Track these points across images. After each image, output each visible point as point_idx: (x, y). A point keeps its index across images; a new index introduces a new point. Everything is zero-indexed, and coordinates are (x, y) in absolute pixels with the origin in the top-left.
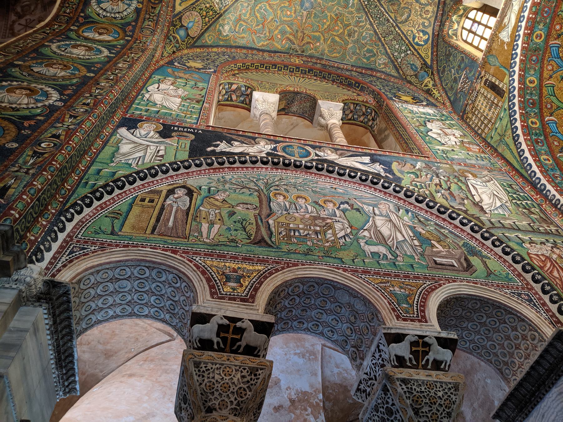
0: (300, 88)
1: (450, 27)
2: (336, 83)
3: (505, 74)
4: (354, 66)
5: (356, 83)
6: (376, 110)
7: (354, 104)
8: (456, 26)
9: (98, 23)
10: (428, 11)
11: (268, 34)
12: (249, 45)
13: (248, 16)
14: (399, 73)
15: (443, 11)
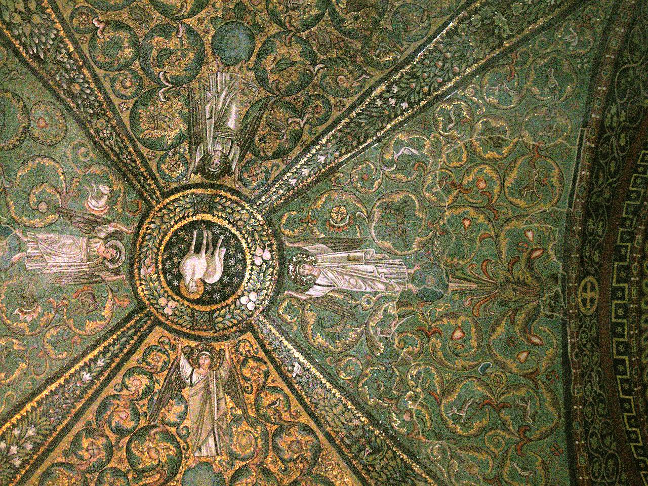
4: (586, 115)
11: (522, 392)
12: (563, 446)
13: (483, 457)
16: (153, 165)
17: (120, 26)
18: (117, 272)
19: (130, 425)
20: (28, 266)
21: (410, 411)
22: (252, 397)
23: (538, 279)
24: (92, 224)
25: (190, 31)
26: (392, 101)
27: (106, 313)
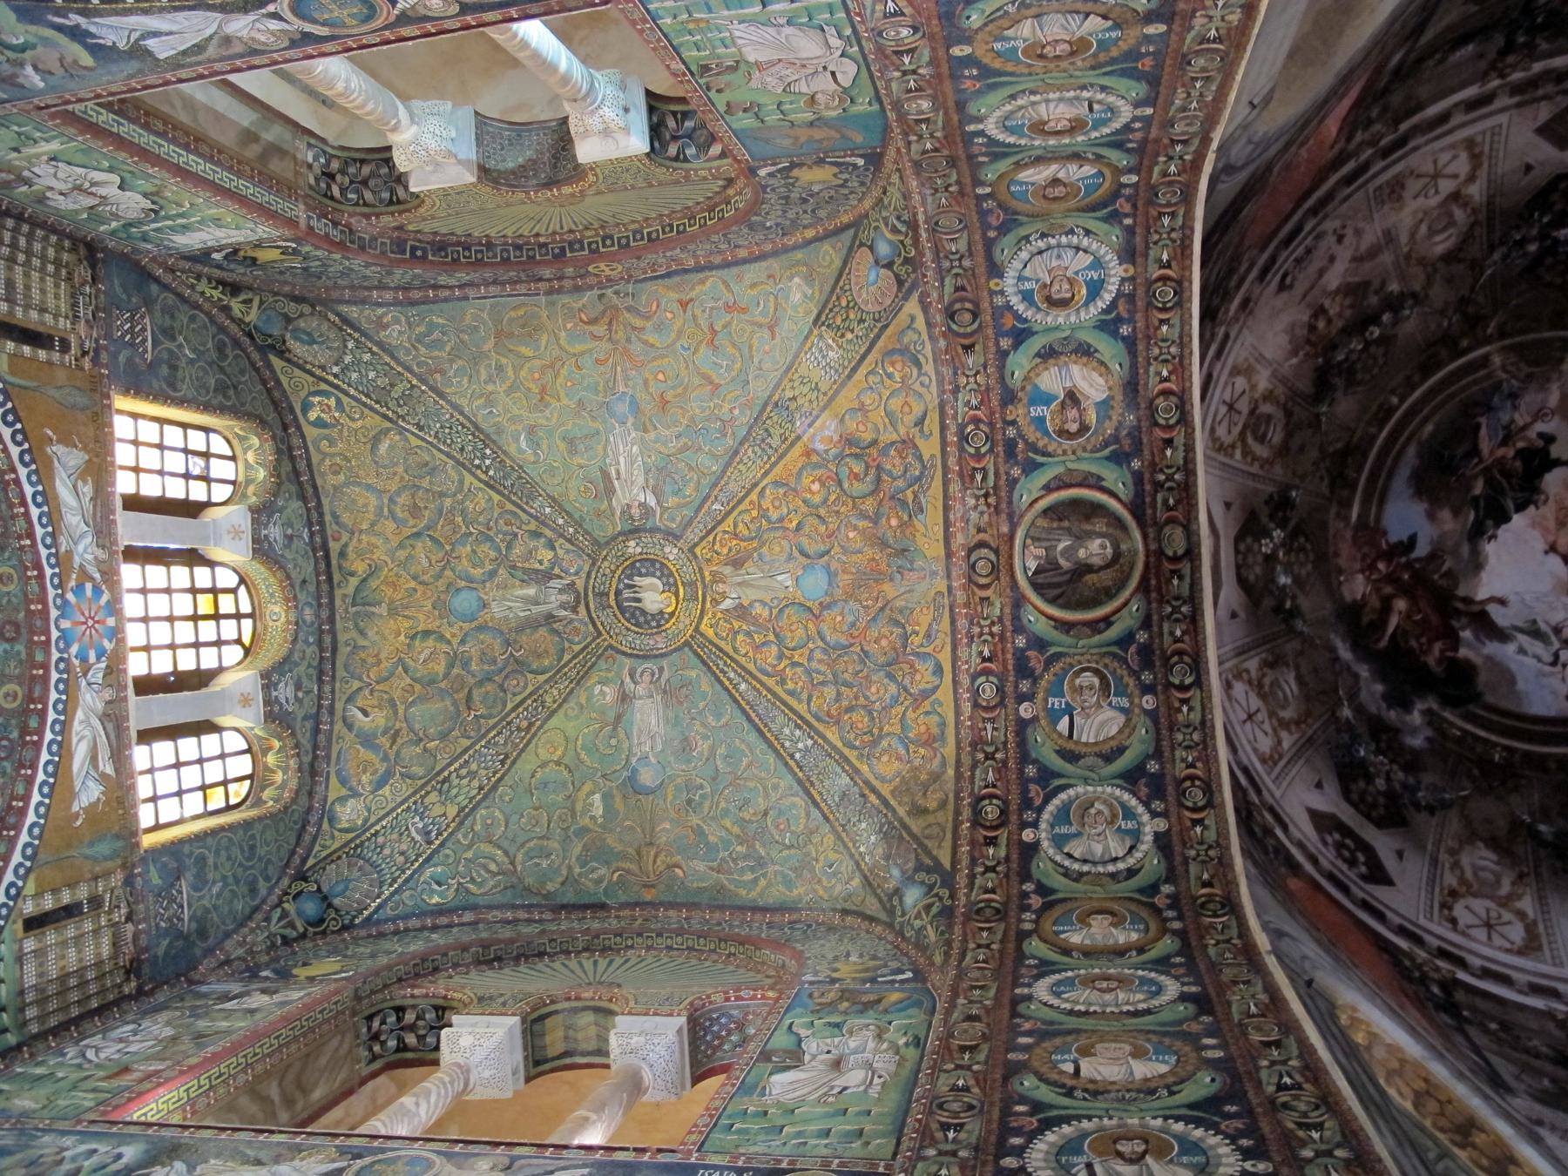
0: (548, 200)
1: (259, 451)
2: (480, 244)
3: (12, 372)
4: (459, 299)
5: (424, 257)
6: (329, 202)
7: (399, 202)
8: (250, 456)
9: (1078, 210)
10: (336, 473)
11: (698, 312)
12: (735, 270)
13: (755, 342)
14: (338, 314)
15: (300, 484)
16: (577, 648)
17: (469, 698)
18: (661, 670)
19: (774, 649)
20: (659, 748)
21: (731, 410)
22: (743, 544)
23: (604, 312)
24: (624, 698)
25: (463, 642)
26: (488, 462)
27: (693, 674)
